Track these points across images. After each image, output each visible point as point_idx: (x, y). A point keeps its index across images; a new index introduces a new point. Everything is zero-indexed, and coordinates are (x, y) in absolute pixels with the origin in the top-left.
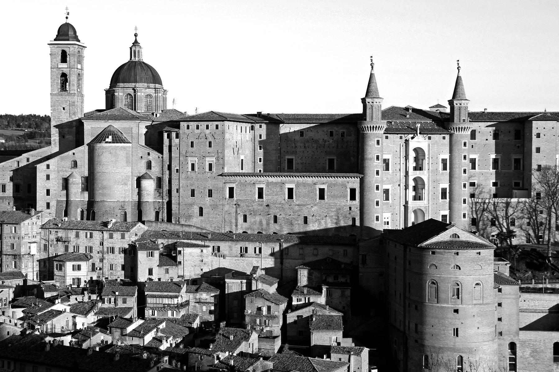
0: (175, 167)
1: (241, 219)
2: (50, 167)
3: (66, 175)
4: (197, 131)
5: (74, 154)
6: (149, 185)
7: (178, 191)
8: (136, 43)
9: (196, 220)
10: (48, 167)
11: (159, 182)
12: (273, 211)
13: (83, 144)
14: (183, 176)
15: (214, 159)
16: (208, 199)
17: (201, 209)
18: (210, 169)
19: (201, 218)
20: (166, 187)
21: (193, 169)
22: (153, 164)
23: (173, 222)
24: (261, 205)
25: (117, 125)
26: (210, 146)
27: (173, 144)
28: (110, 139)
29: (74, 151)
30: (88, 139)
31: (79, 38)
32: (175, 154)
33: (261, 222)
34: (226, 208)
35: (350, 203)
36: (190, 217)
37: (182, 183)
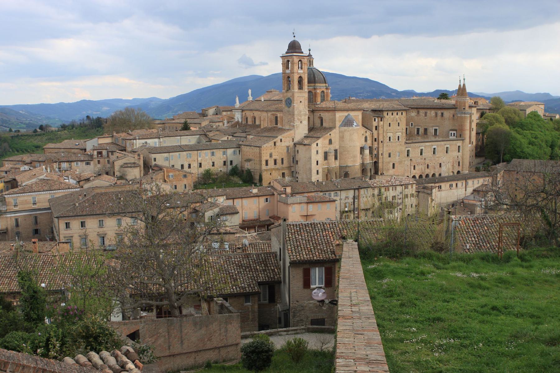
0: (381, 139)
1: (413, 168)
3: (327, 150)
4: (392, 117)
6: (367, 152)
7: (382, 154)
10: (317, 145)
12: (427, 162)
14: (385, 145)
15: (400, 133)
17: (394, 164)
18: (398, 140)
19: (394, 170)
20: (375, 152)
21: (390, 140)
22: (368, 138)
24: (422, 159)
28: (355, 124)
30: (338, 124)
31: (303, 50)
32: (381, 131)
33: (422, 169)
34: (406, 162)
35: (458, 154)
36: (388, 170)
37: (384, 150)
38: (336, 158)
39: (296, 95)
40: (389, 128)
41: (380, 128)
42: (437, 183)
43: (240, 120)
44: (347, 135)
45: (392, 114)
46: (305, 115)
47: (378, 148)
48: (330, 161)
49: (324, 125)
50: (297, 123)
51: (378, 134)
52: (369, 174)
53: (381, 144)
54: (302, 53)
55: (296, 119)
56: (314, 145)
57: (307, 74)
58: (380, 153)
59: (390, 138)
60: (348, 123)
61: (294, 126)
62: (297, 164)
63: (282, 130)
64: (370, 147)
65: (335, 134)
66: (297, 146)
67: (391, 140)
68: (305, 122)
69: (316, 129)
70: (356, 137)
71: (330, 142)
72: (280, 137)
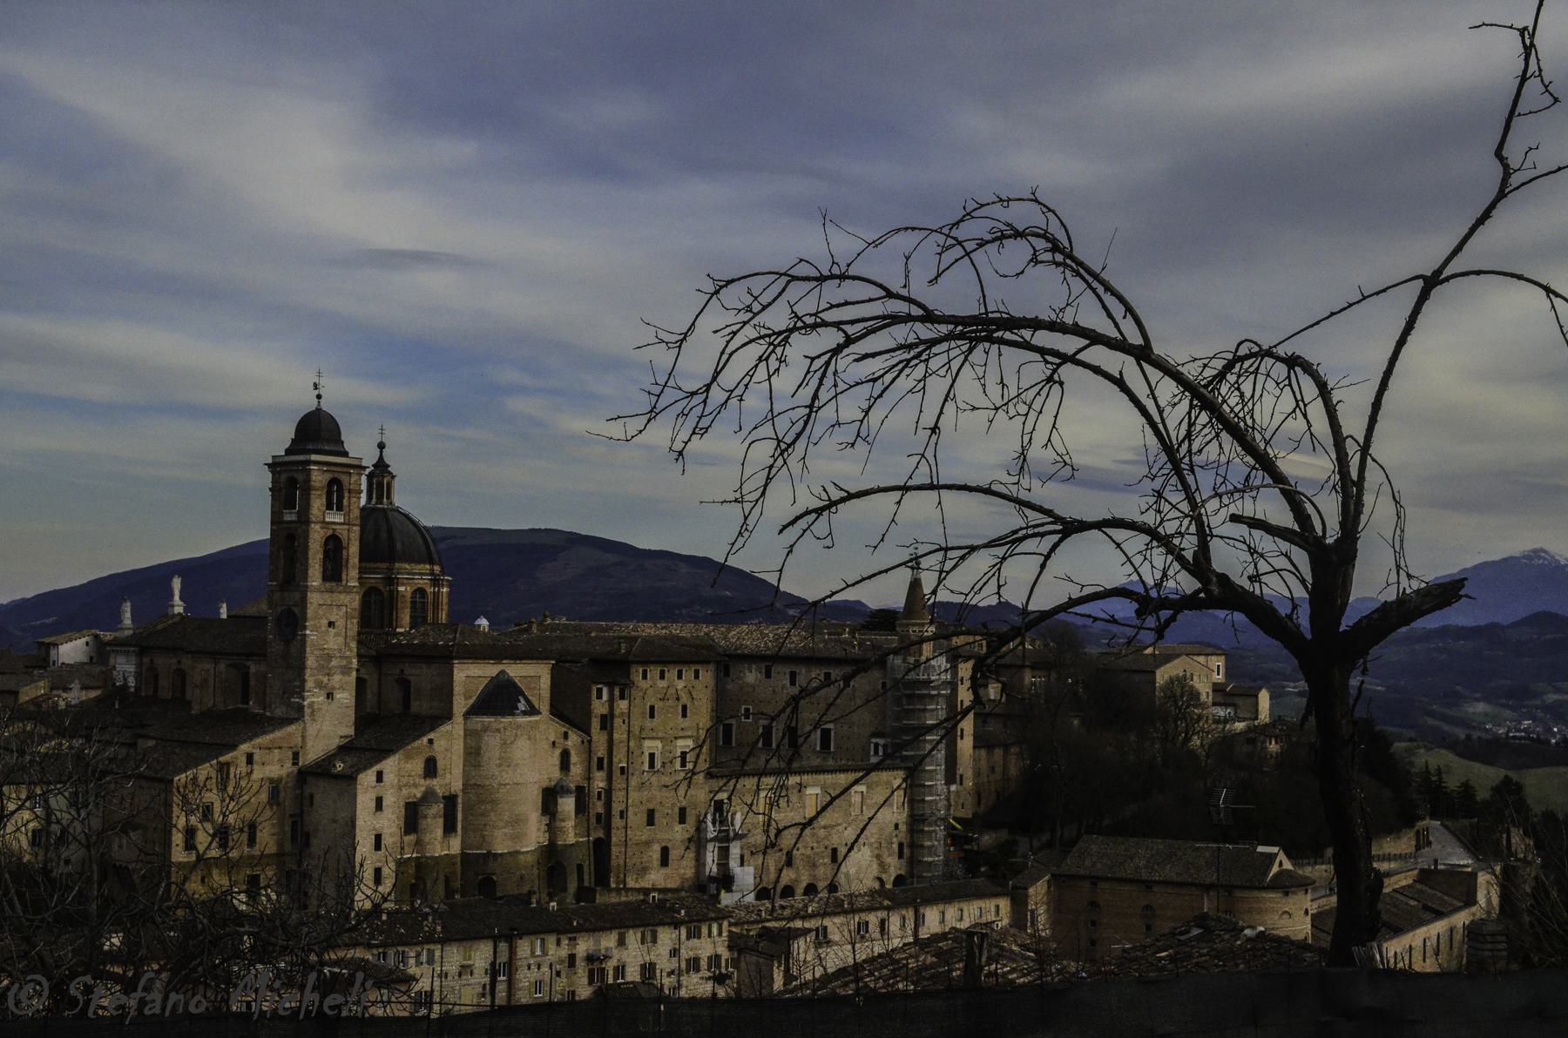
0: (620, 760)
2: (385, 778)
4: (662, 684)
5: (431, 741)
6: (567, 804)
7: (622, 814)
8: (381, 466)
9: (657, 877)
10: (380, 777)
11: (581, 795)
13: (448, 716)
14: (634, 781)
16: (678, 828)
17: (665, 852)
19: (664, 871)
21: (652, 765)
22: (574, 758)
23: (613, 885)
25: (516, 671)
26: (684, 715)
27: (617, 712)
28: (522, 706)
29: (432, 735)
30: (460, 705)
36: (644, 870)
37: (633, 799)
38: (449, 828)
39: (314, 599)
40: (648, 723)
41: (618, 721)
42: (813, 916)
43: (132, 682)
44: (492, 743)
45: (662, 677)
46: (345, 670)
47: (609, 791)
48: (427, 838)
49: (415, 706)
50: (314, 697)
51: (610, 742)
52: (572, 886)
53: (618, 782)
54: (345, 454)
55: (310, 684)
56: (367, 778)
57: (357, 528)
58: (617, 807)
59: (652, 756)
60: (500, 699)
61: (301, 708)
62: (308, 845)
63: (260, 724)
64: (580, 789)
65: (448, 742)
66: (310, 779)
67: (658, 765)
68: (346, 697)
69: (388, 722)
70: (528, 755)
71: (431, 768)
72: (245, 747)
